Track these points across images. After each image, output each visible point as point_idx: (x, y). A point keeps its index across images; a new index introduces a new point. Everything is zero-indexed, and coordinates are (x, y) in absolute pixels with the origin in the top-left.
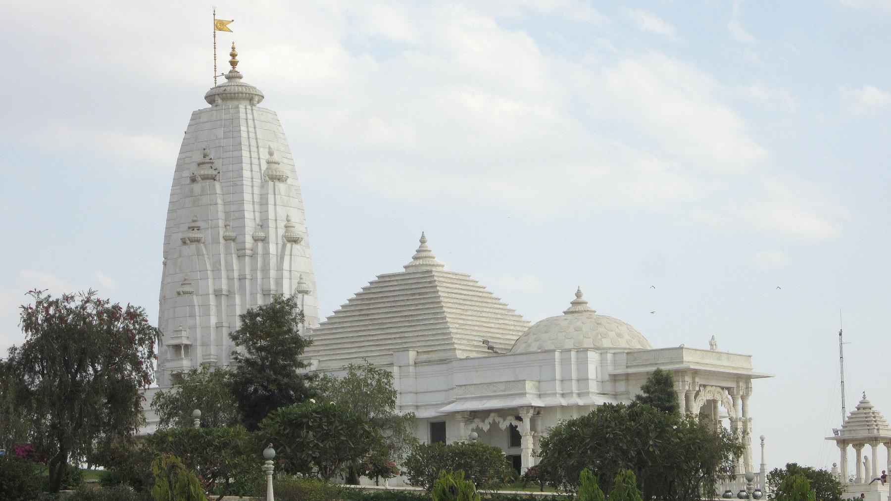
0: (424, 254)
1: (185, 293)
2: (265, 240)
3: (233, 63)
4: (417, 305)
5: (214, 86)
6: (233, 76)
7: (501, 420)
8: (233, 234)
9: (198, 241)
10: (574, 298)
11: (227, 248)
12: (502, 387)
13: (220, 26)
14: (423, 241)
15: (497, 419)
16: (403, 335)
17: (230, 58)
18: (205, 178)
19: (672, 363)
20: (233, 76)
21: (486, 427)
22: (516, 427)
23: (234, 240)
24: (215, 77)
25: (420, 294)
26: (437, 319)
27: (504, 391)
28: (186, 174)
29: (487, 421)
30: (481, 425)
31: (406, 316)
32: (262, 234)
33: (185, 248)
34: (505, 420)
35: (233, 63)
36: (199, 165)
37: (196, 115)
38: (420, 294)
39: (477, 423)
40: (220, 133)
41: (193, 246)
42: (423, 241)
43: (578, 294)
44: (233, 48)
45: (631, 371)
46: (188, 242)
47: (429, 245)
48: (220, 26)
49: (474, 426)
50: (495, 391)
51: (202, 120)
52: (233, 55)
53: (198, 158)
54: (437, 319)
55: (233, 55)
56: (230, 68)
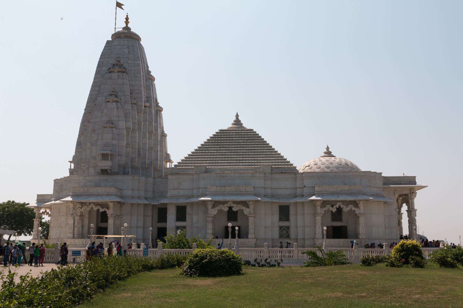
2: (150, 107)
4: (253, 145)
5: (113, 32)
6: (127, 28)
7: (344, 207)
10: (326, 151)
14: (237, 116)
15: (342, 206)
19: (401, 184)
20: (127, 28)
21: (334, 210)
22: (355, 211)
28: (105, 69)
29: (335, 207)
30: (331, 209)
31: (250, 150)
32: (148, 104)
34: (347, 206)
38: (252, 140)
39: (328, 207)
40: (126, 51)
41: (115, 104)
42: (237, 116)
43: (328, 148)
44: (127, 16)
47: (240, 118)
49: (326, 209)
52: (127, 19)
53: (113, 61)
55: (127, 19)
56: (125, 25)
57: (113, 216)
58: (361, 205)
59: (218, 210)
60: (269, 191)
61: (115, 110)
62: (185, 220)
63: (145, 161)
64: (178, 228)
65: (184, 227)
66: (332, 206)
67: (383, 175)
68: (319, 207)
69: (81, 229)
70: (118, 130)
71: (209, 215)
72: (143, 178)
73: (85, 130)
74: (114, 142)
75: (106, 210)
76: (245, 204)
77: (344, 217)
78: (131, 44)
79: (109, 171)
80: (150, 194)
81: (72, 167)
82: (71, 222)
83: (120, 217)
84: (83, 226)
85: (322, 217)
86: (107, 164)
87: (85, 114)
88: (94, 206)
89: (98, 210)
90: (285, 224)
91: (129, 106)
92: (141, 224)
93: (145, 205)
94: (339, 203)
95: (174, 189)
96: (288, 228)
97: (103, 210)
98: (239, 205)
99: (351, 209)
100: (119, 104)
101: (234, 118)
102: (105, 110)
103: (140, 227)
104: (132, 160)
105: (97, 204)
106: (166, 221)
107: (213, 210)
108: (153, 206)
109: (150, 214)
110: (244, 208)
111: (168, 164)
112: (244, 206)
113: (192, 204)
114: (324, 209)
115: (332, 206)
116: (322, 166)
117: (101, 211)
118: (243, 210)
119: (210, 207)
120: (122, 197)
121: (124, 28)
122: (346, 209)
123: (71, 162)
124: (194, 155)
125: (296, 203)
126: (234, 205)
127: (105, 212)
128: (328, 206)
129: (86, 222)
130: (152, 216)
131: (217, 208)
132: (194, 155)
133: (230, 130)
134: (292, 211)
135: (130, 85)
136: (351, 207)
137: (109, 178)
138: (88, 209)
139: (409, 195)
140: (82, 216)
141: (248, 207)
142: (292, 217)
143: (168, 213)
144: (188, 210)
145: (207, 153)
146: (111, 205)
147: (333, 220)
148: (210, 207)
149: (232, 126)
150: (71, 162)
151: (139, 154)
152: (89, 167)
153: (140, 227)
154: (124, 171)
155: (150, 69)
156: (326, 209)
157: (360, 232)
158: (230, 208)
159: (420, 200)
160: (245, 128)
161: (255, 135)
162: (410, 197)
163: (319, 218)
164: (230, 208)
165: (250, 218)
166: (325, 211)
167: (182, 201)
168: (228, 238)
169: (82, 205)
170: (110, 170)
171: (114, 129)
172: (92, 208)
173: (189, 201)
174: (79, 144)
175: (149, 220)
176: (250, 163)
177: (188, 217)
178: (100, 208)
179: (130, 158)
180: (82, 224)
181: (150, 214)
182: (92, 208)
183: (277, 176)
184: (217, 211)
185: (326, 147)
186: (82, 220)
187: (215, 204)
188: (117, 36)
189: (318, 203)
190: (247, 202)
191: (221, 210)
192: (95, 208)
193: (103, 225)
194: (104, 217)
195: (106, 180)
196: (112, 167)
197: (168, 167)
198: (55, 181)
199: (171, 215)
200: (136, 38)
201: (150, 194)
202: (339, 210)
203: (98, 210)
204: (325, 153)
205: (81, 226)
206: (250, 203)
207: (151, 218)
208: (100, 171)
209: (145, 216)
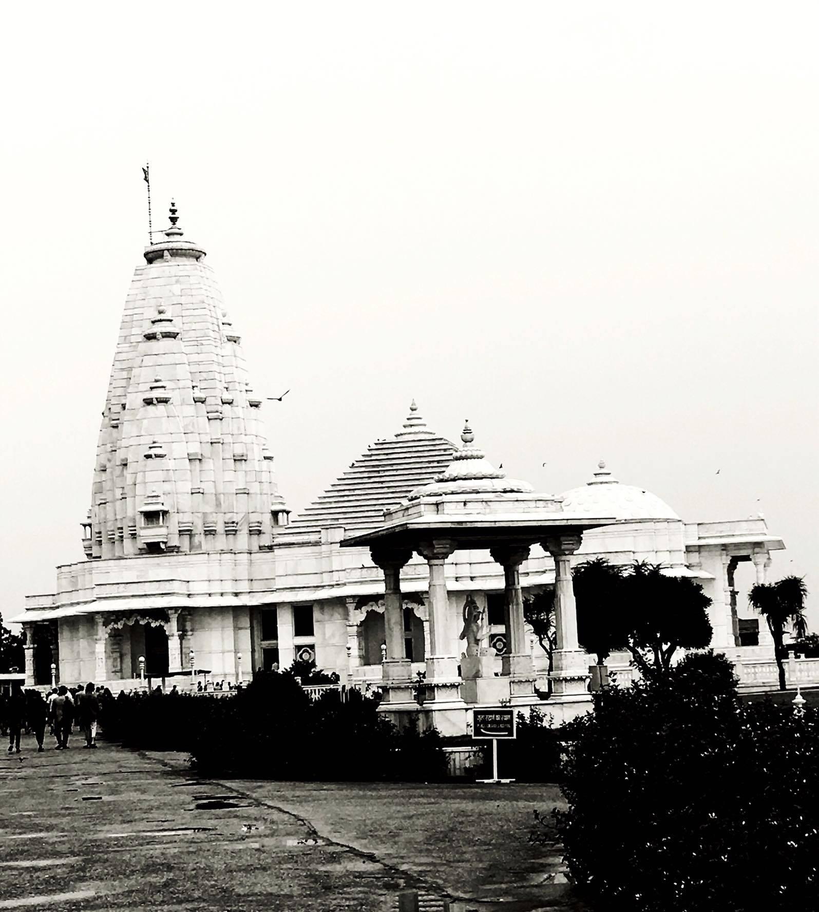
1: (157, 456)
3: (174, 220)
8: (202, 395)
9: (165, 401)
11: (196, 409)
17: (170, 214)
18: (167, 335)
33: (150, 408)
35: (174, 220)
36: (153, 322)
38: (438, 462)
41: (161, 407)
44: (173, 205)
45: (702, 542)
46: (155, 402)
56: (170, 224)
59: (367, 612)
62: (310, 633)
64: (298, 648)
65: (312, 647)
71: (351, 623)
75: (162, 624)
79: (163, 546)
80: (244, 587)
82: (101, 648)
83: (190, 633)
84: (121, 657)
91: (191, 410)
100: (169, 406)
106: (275, 637)
110: (414, 606)
111: (280, 514)
113: (323, 603)
117: (153, 625)
118: (412, 609)
119: (351, 607)
123: (85, 526)
127: (161, 627)
129: (127, 648)
131: (364, 609)
138: (131, 623)
140: (115, 636)
141: (423, 604)
144: (316, 615)
148: (351, 607)
150: (85, 526)
151: (218, 504)
153: (229, 651)
169: (117, 617)
170: (165, 543)
171: (163, 460)
175: (245, 635)
177: (316, 627)
178: (150, 621)
179: (200, 515)
182: (137, 622)
197: (281, 523)
199: (285, 625)
208: (145, 546)
209: (237, 628)
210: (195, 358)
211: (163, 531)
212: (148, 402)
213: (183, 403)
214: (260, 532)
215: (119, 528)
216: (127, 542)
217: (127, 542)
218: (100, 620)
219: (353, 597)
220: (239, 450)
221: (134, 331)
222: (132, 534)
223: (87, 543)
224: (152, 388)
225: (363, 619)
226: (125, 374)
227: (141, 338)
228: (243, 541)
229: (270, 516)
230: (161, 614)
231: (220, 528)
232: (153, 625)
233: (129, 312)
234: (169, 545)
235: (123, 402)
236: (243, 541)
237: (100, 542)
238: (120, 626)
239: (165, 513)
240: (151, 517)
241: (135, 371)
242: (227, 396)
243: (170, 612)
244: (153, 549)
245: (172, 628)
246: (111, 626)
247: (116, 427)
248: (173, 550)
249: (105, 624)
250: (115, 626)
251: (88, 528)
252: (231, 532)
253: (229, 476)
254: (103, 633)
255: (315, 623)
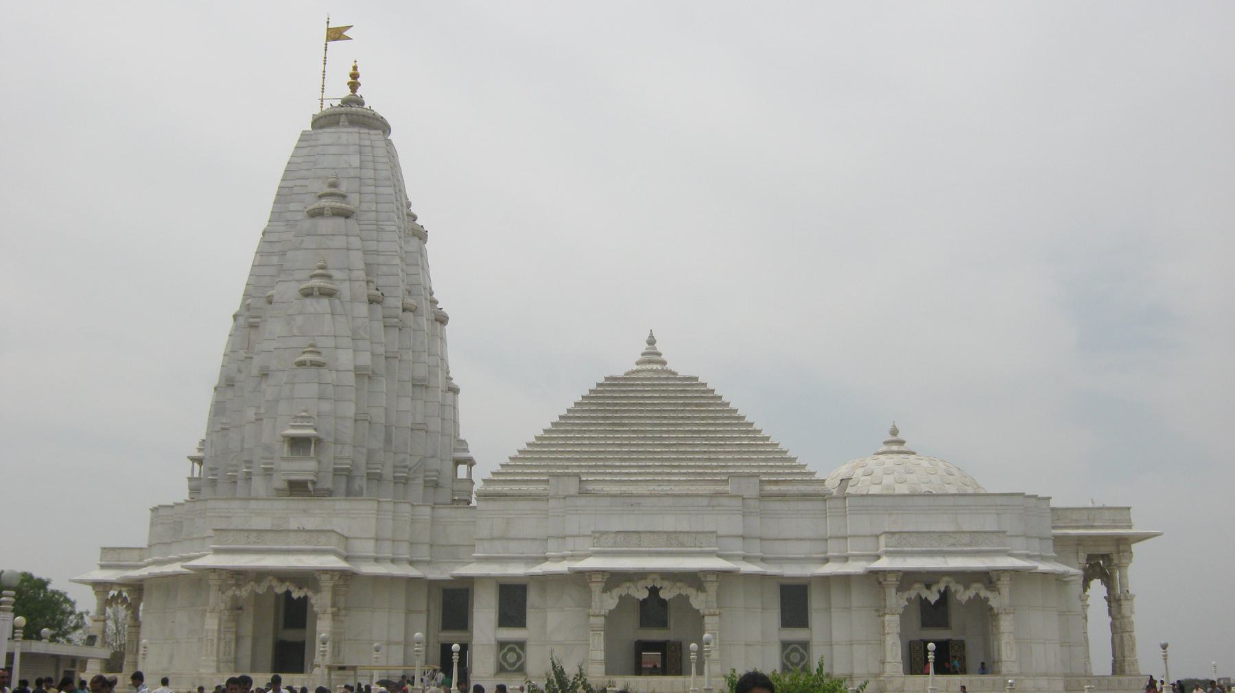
0: (656, 358)
3: (354, 86)
4: (703, 418)
5: (317, 111)
7: (961, 588)
10: (890, 438)
12: (966, 539)
13: (336, 34)
14: (651, 342)
16: (712, 456)
17: (350, 80)
21: (933, 597)
22: (987, 599)
23: (378, 303)
24: (322, 100)
25: (697, 405)
26: (755, 439)
27: (970, 545)
29: (934, 589)
30: (925, 594)
31: (694, 432)
33: (308, 301)
34: (967, 587)
35: (354, 86)
37: (304, 137)
38: (697, 405)
39: (917, 590)
40: (355, 161)
42: (651, 342)
43: (894, 432)
44: (355, 68)
46: (316, 293)
47: (659, 347)
48: (336, 34)
50: (953, 545)
51: (320, 142)
52: (355, 76)
54: (755, 439)
55: (355, 76)
56: (347, 92)
57: (330, 610)
58: (1004, 584)
59: (621, 597)
60: (756, 549)
61: (328, 317)
63: (404, 460)
64: (502, 645)
65: (522, 645)
66: (928, 587)
67: (1054, 503)
68: (894, 590)
69: (233, 646)
70: (334, 373)
71: (597, 612)
72: (406, 508)
73: (240, 371)
74: (326, 406)
75: (310, 594)
76: (695, 579)
77: (954, 619)
78: (368, 143)
79: (310, 487)
80: (424, 553)
81: (196, 475)
82: (212, 623)
83: (343, 612)
84: (238, 639)
85: (902, 616)
86: (303, 468)
87: (236, 328)
88: (275, 583)
89: (288, 593)
90: (797, 634)
91: (363, 309)
92: (398, 634)
93: (411, 581)
94: (946, 579)
95: (493, 539)
96: (805, 645)
97: (301, 594)
98: (679, 584)
99: (977, 594)
100: (337, 302)
101: (644, 347)
102: (299, 320)
103: (398, 643)
104: (371, 453)
105: (282, 576)
107: (606, 596)
108: (432, 584)
109: (424, 608)
110: (691, 592)
112: (690, 586)
114: (906, 595)
115: (928, 587)
116: (888, 480)
117: (295, 595)
118: (687, 597)
119: (596, 588)
120: (346, 559)
121: (346, 102)
122: (963, 595)
123: (193, 459)
124: (544, 446)
125: (826, 580)
126: (666, 584)
127: (305, 600)
128: (917, 586)
129: (247, 628)
130: (428, 610)
131: (617, 592)
132: (544, 446)
133: (634, 379)
134: (815, 602)
135: (365, 252)
136: (978, 589)
137: (313, 505)
139: (1115, 556)
140: (237, 608)
142: (815, 618)
143: (476, 605)
144: (532, 598)
145: (578, 438)
146: (326, 583)
147: (925, 624)
148: (596, 588)
149: (639, 367)
150: (193, 459)
151: (388, 440)
152: (249, 473)
153: (398, 643)
154: (349, 482)
155: (414, 210)
156: (912, 594)
157: (1004, 657)
158: (654, 591)
159: (1138, 572)
160: (674, 373)
161: (704, 392)
162: (1116, 562)
163: (892, 622)
164: (654, 591)
165: (707, 619)
166: (909, 600)
167: (516, 570)
168: (690, 673)
170: (314, 483)
171: (323, 371)
172: (271, 588)
173: (538, 569)
174: (218, 409)
176: (699, 467)
177: (531, 617)
179: (364, 451)
180: (237, 633)
181: (423, 606)
182: (271, 588)
183: (775, 505)
184: (617, 600)
185: (890, 427)
186: (236, 620)
187: (614, 579)
188: (323, 121)
189: (892, 579)
190: (700, 575)
191: (628, 595)
192: (280, 589)
193: (291, 635)
194: (295, 613)
195: (305, 511)
196: (317, 474)
198: (155, 510)
200: (378, 124)
201: (424, 553)
202: (945, 596)
203: (288, 593)
204: (886, 443)
205: (233, 637)
206: (709, 578)
207: (424, 616)
209: (409, 612)
210: (372, 245)
211: (311, 465)
212: (307, 293)
213: (353, 299)
214: (436, 485)
215: (246, 462)
216: (258, 484)
217: (258, 484)
218: (213, 581)
219: (602, 572)
220: (421, 371)
221: (292, 207)
222: (266, 469)
223: (195, 483)
224: (313, 277)
225: (613, 607)
226: (275, 260)
227: (299, 217)
228: (417, 489)
229: (451, 464)
230: (306, 578)
231: (388, 472)
232: (295, 595)
233: (290, 184)
234: (320, 486)
235: (269, 293)
236: (417, 489)
237: (217, 474)
238: (244, 592)
239: (318, 441)
240: (298, 444)
241: (290, 254)
242: (410, 301)
243: (325, 577)
244: (297, 488)
245: (320, 601)
246: (230, 593)
247: (254, 326)
248: (329, 493)
249: (222, 590)
250: (238, 593)
251: (197, 466)
252: (403, 482)
253: (406, 404)
254: (217, 599)
255: (528, 610)
